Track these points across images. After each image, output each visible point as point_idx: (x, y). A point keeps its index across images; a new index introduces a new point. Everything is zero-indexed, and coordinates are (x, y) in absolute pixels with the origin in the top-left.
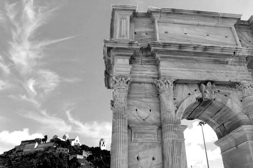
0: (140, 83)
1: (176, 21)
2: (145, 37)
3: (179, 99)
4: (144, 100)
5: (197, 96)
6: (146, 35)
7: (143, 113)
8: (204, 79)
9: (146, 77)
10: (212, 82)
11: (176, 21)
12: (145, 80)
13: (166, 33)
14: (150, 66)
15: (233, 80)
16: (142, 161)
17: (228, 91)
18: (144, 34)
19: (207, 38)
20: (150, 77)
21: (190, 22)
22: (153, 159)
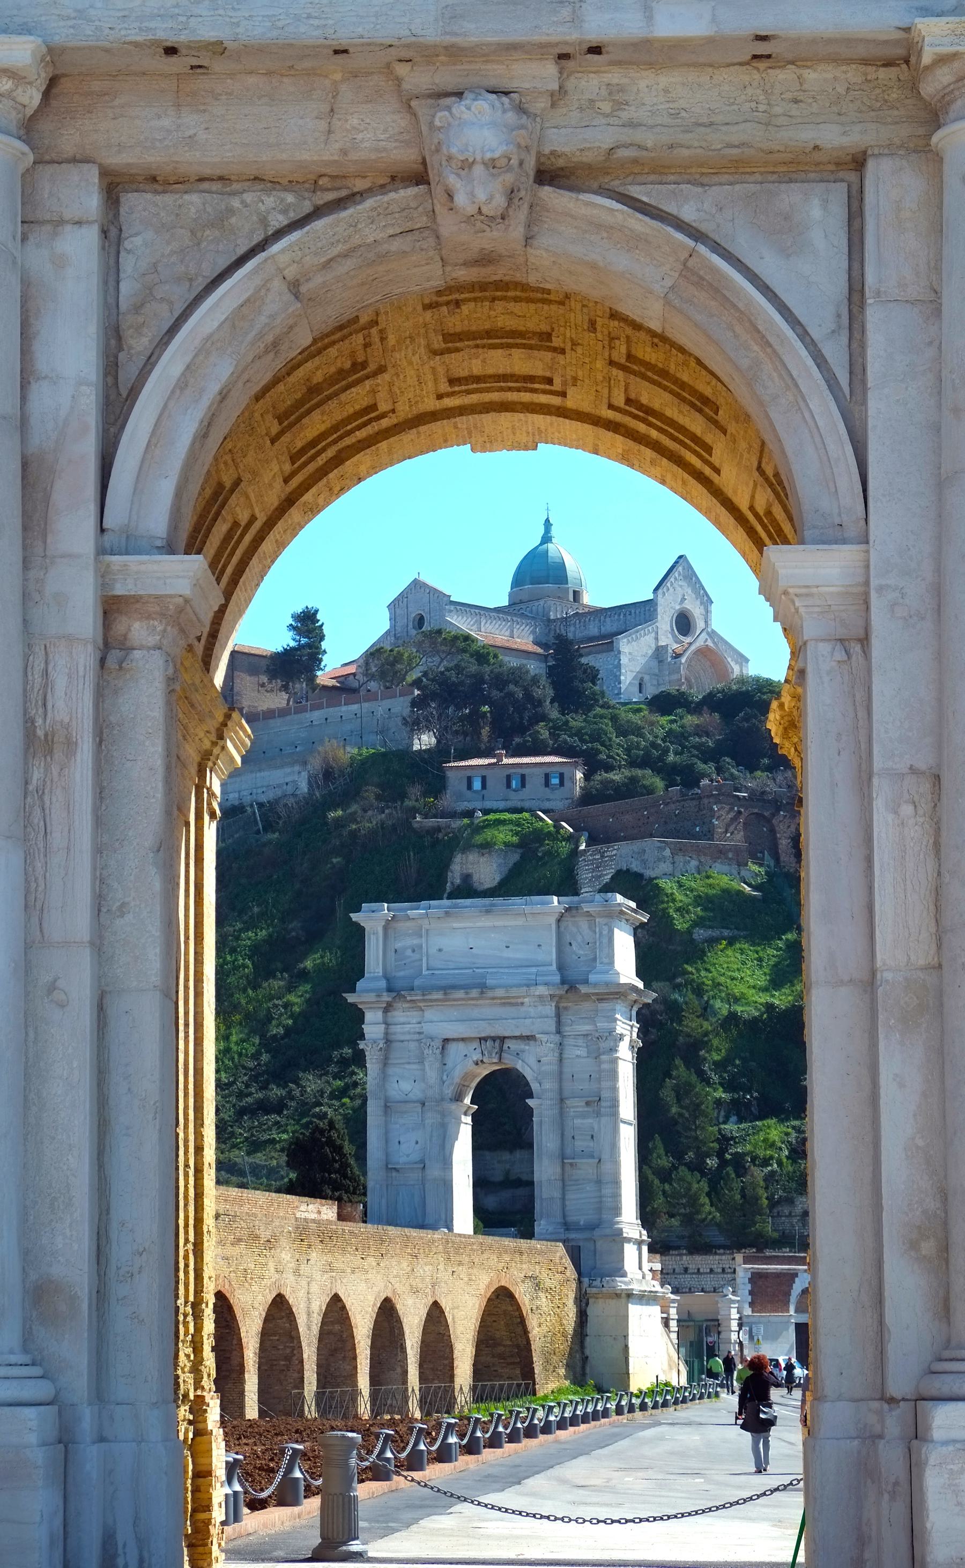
0: (402, 1041)
1: (455, 925)
2: (410, 957)
3: (450, 1064)
4: (407, 1066)
5: (475, 1059)
6: (412, 954)
7: (406, 1086)
8: (483, 1035)
9: (409, 1033)
10: (494, 1039)
11: (455, 925)
12: (407, 1037)
13: (440, 950)
14: (415, 1013)
15: (526, 1033)
16: (403, 1146)
17: (522, 1047)
18: (409, 952)
19: (508, 954)
20: (415, 1033)
21: (479, 924)
22: (417, 1143)
